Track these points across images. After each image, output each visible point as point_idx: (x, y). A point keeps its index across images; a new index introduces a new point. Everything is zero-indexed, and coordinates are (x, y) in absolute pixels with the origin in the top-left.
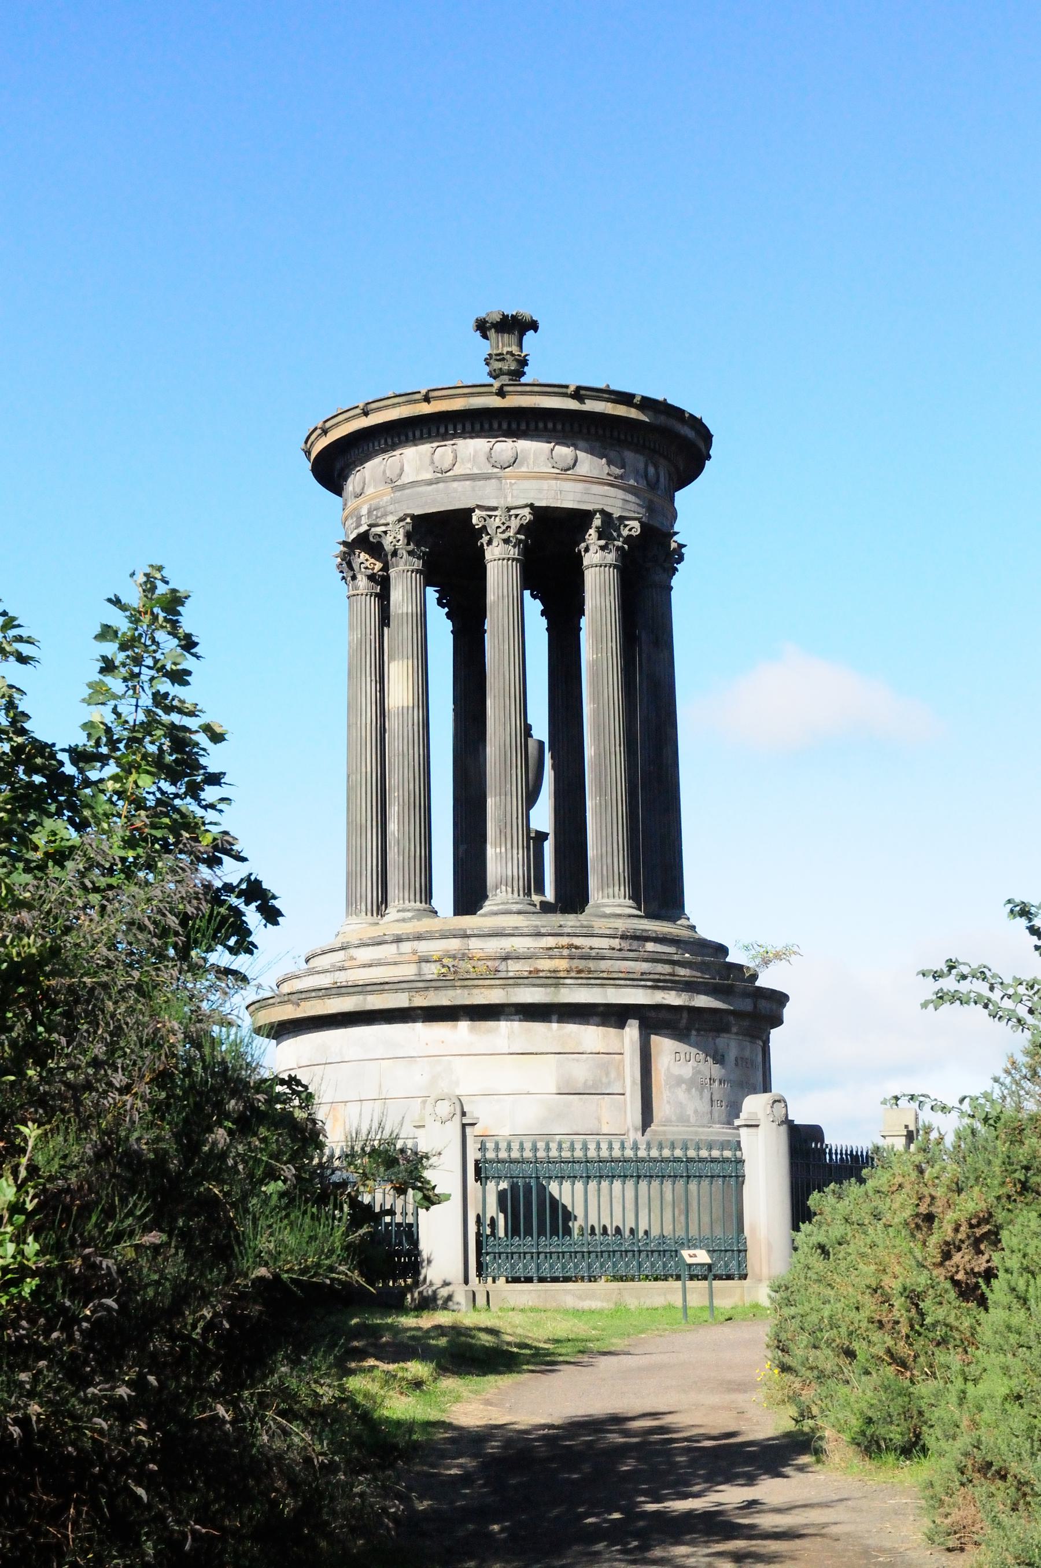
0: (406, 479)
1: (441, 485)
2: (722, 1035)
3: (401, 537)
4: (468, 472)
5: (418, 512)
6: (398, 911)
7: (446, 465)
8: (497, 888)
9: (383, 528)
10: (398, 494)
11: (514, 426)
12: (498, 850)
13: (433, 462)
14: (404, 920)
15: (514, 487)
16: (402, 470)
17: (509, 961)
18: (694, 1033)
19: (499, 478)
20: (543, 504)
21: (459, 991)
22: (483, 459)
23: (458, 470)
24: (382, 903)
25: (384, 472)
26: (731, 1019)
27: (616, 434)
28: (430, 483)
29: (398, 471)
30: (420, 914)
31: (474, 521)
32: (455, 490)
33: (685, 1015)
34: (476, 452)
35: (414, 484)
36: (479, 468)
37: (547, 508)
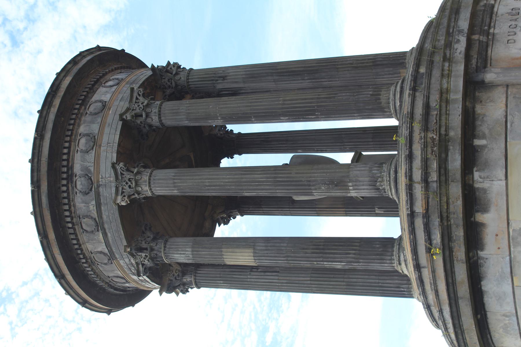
0: (106, 251)
1: (106, 226)
2: (495, 9)
3: (143, 255)
4: (95, 207)
5: (125, 243)
6: (400, 264)
7: (93, 223)
8: (378, 189)
9: (140, 266)
10: (117, 256)
11: (65, 176)
12: (351, 188)
13: (92, 232)
14: (405, 261)
15: (104, 176)
16: (101, 252)
17: (430, 180)
18: (491, 31)
19: (98, 186)
20: (115, 155)
21: (452, 221)
22: (87, 198)
23: (95, 214)
24: (395, 273)
25: (106, 264)
26: (482, 4)
27: (78, 106)
28: (105, 235)
29: (102, 255)
30: (401, 248)
31: (123, 204)
32: (108, 216)
33: (476, 37)
34: (83, 202)
35: (107, 244)
36: (92, 200)
37: (118, 153)
